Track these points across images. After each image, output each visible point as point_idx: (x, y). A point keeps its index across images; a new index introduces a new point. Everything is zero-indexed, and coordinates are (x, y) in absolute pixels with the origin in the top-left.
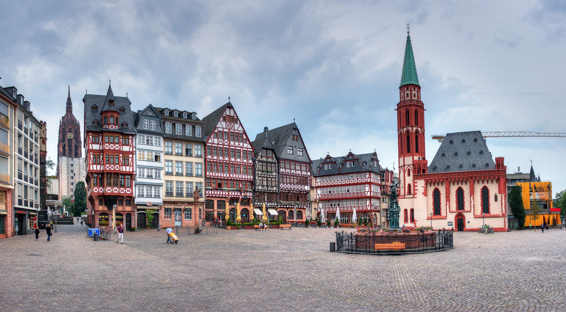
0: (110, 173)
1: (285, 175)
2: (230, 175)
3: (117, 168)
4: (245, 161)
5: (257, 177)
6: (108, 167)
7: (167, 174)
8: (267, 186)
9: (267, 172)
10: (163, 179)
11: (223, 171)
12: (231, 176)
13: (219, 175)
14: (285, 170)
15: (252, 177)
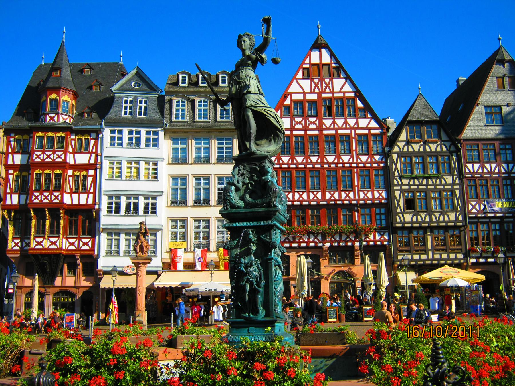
0: (40, 210)
1: (482, 178)
2: (324, 196)
3: (56, 197)
4: (364, 158)
5: (397, 194)
6: (37, 198)
7: (174, 203)
8: (430, 213)
9: (427, 178)
10: (165, 213)
11: (306, 188)
12: (328, 196)
13: (297, 196)
14: (482, 166)
15: (384, 194)
